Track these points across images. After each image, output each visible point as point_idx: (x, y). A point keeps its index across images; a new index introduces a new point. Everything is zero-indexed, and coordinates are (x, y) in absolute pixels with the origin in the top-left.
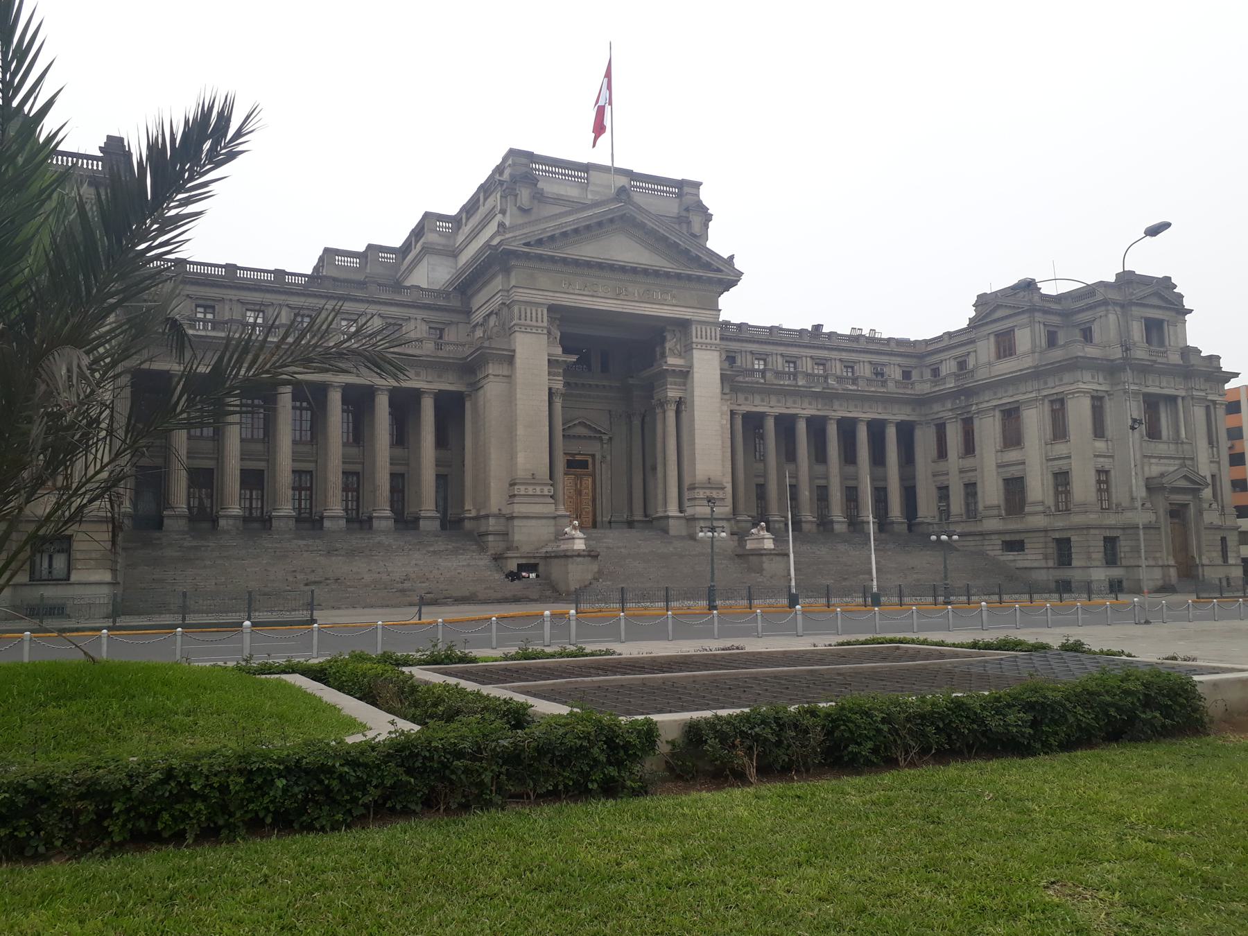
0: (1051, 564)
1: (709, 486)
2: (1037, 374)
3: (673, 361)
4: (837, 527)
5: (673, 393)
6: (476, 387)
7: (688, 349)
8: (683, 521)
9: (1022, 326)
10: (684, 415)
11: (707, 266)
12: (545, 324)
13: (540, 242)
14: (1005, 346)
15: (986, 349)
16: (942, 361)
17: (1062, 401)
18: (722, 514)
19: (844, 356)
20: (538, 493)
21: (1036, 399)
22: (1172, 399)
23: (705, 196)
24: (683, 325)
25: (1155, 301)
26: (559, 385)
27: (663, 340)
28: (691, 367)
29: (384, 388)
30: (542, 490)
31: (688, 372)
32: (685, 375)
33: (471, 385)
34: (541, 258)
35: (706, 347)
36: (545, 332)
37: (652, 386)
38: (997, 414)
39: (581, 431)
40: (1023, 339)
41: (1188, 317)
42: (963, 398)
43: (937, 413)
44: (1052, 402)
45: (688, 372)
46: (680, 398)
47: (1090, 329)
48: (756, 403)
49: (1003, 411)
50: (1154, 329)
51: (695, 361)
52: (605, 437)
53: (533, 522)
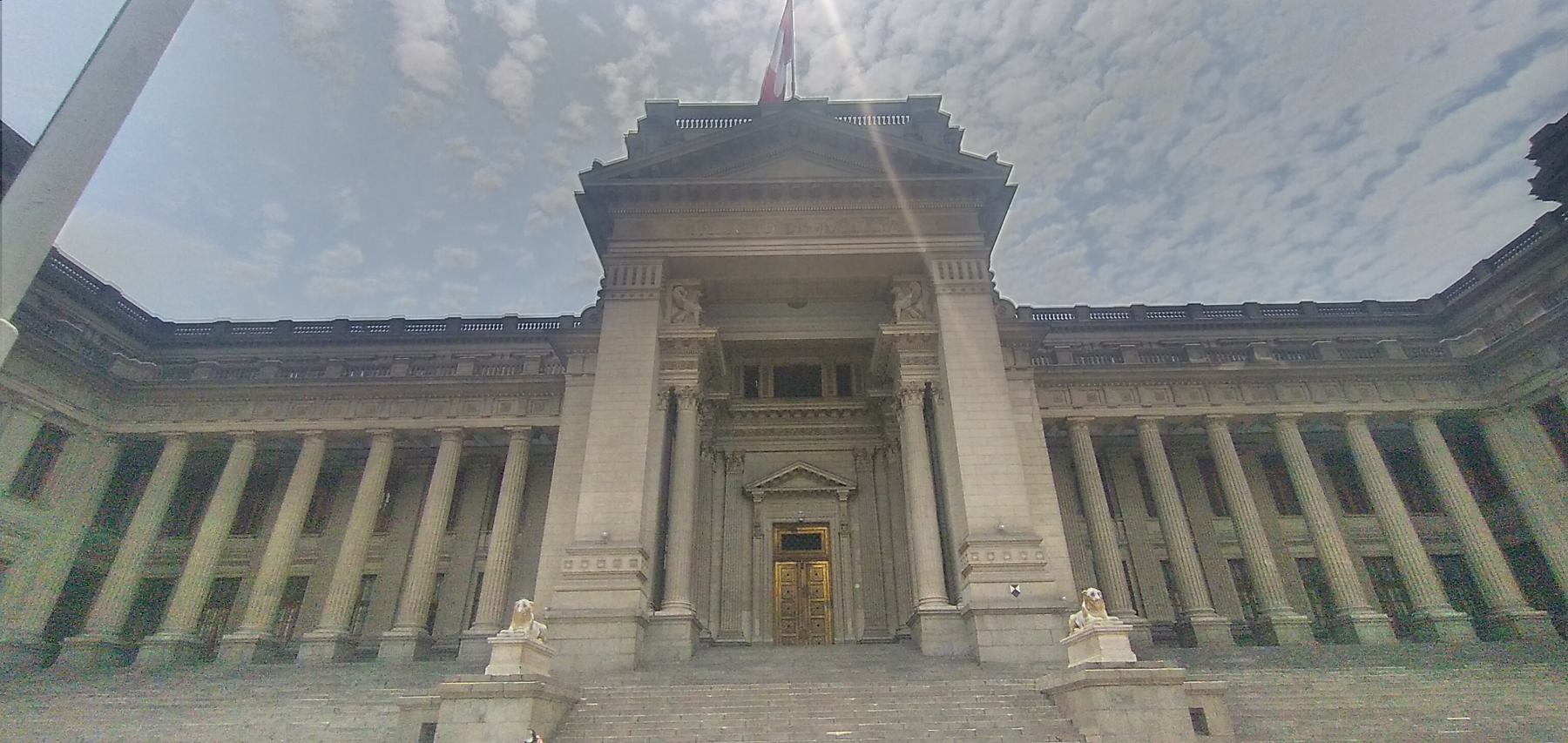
1: (1001, 538)
4: (1368, 633)
5: (911, 376)
8: (956, 622)
10: (939, 410)
11: (942, 168)
12: (658, 285)
13: (648, 173)
18: (1041, 599)
20: (609, 568)
26: (688, 380)
28: (938, 327)
29: (449, 430)
30: (618, 563)
31: (937, 334)
36: (657, 295)
39: (801, 483)
43: (1528, 380)
45: (937, 334)
46: (928, 384)
48: (1111, 402)
52: (843, 492)
53: (587, 630)
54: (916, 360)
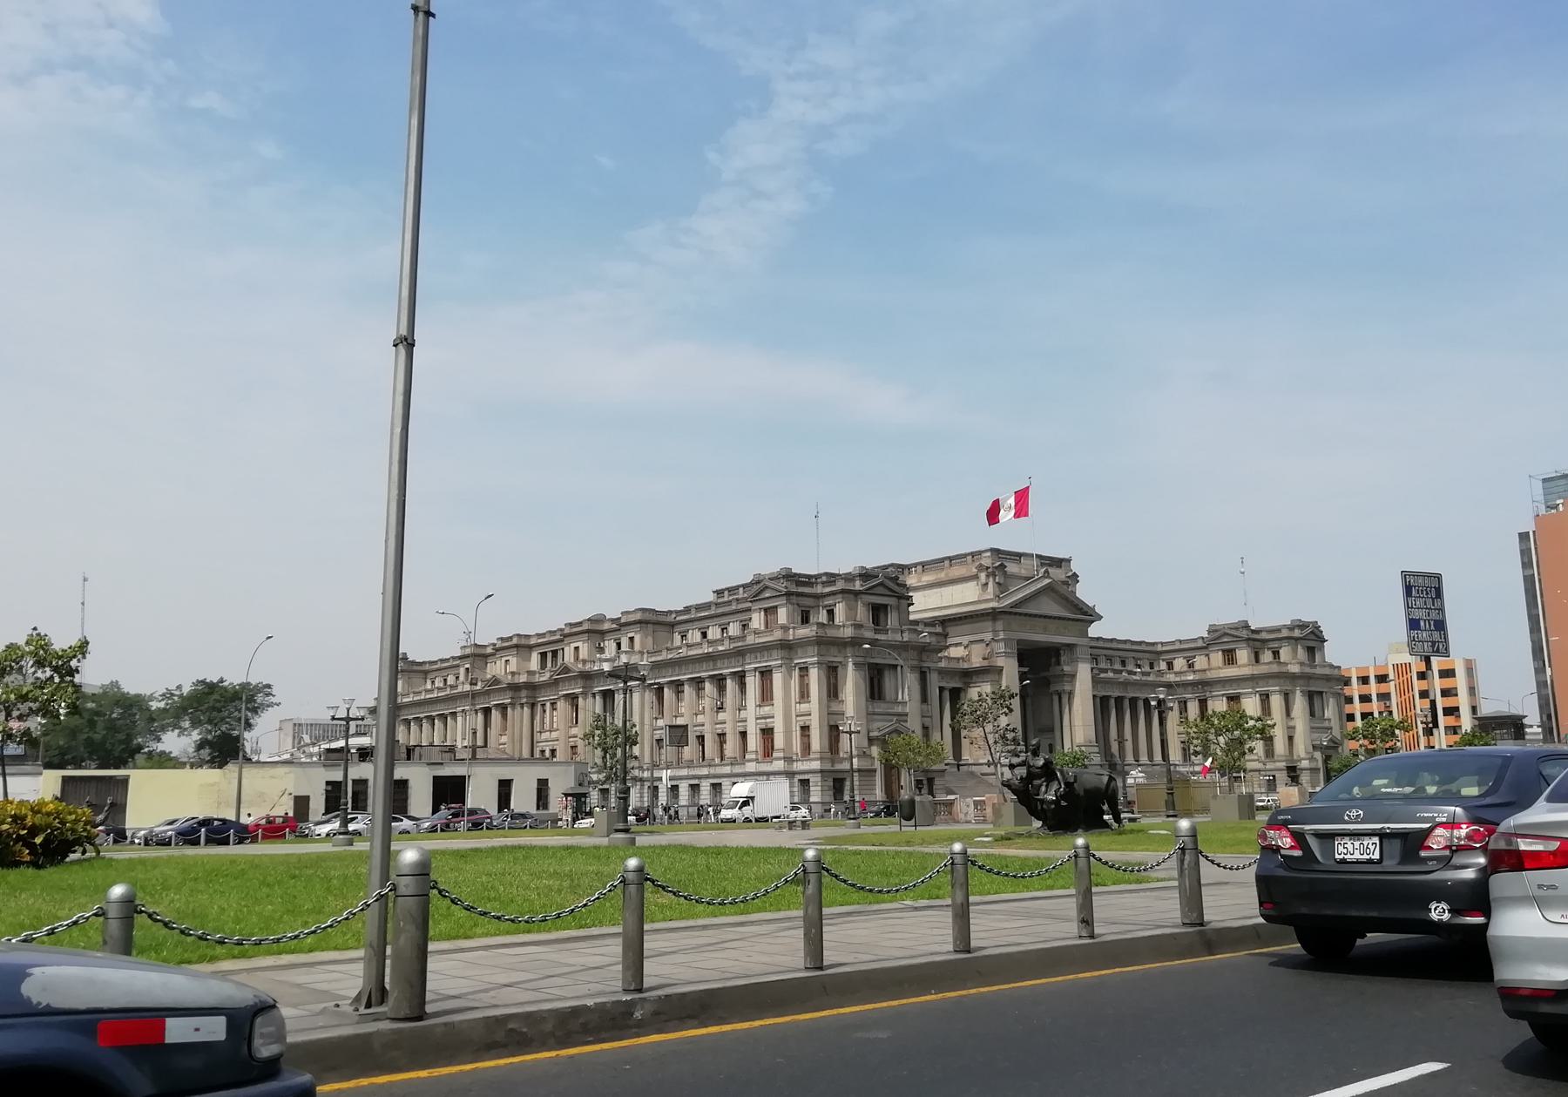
0: (1263, 790)
2: (1253, 679)
3: (1067, 668)
6: (968, 685)
7: (1074, 661)
9: (1240, 648)
11: (1085, 614)
14: (1230, 657)
15: (1217, 658)
16: (1174, 659)
17: (1268, 696)
19: (1121, 653)
21: (1251, 693)
22: (1321, 693)
23: (1075, 567)
24: (1071, 647)
25: (1313, 637)
27: (1058, 655)
32: (1073, 676)
33: (965, 683)
34: (1016, 614)
35: (1084, 660)
37: (1047, 682)
38: (1224, 698)
40: (1243, 655)
41: (1325, 644)
42: (1200, 686)
44: (1260, 695)
47: (1278, 652)
49: (1228, 698)
50: (1311, 651)
51: (1079, 669)
54: (1067, 682)
